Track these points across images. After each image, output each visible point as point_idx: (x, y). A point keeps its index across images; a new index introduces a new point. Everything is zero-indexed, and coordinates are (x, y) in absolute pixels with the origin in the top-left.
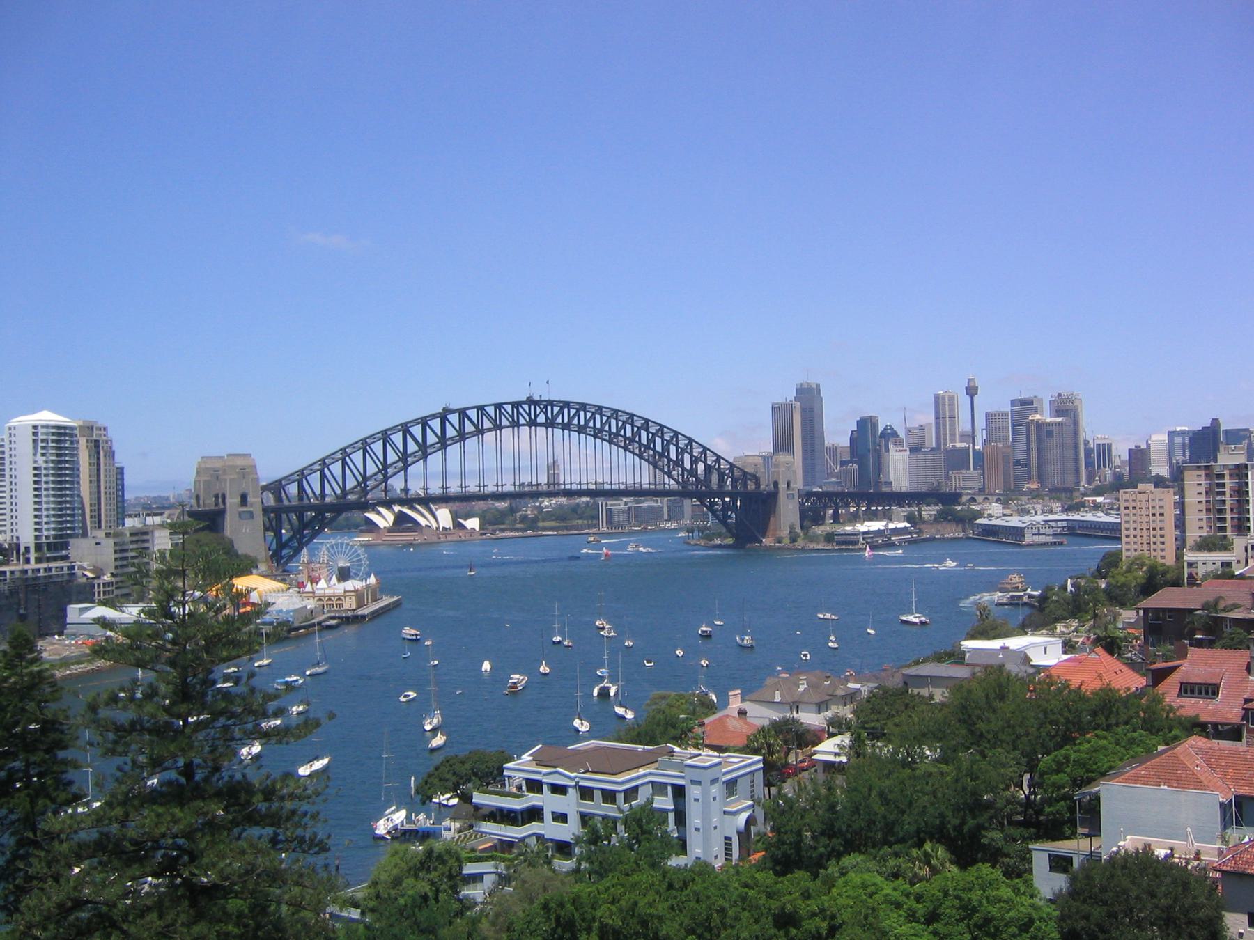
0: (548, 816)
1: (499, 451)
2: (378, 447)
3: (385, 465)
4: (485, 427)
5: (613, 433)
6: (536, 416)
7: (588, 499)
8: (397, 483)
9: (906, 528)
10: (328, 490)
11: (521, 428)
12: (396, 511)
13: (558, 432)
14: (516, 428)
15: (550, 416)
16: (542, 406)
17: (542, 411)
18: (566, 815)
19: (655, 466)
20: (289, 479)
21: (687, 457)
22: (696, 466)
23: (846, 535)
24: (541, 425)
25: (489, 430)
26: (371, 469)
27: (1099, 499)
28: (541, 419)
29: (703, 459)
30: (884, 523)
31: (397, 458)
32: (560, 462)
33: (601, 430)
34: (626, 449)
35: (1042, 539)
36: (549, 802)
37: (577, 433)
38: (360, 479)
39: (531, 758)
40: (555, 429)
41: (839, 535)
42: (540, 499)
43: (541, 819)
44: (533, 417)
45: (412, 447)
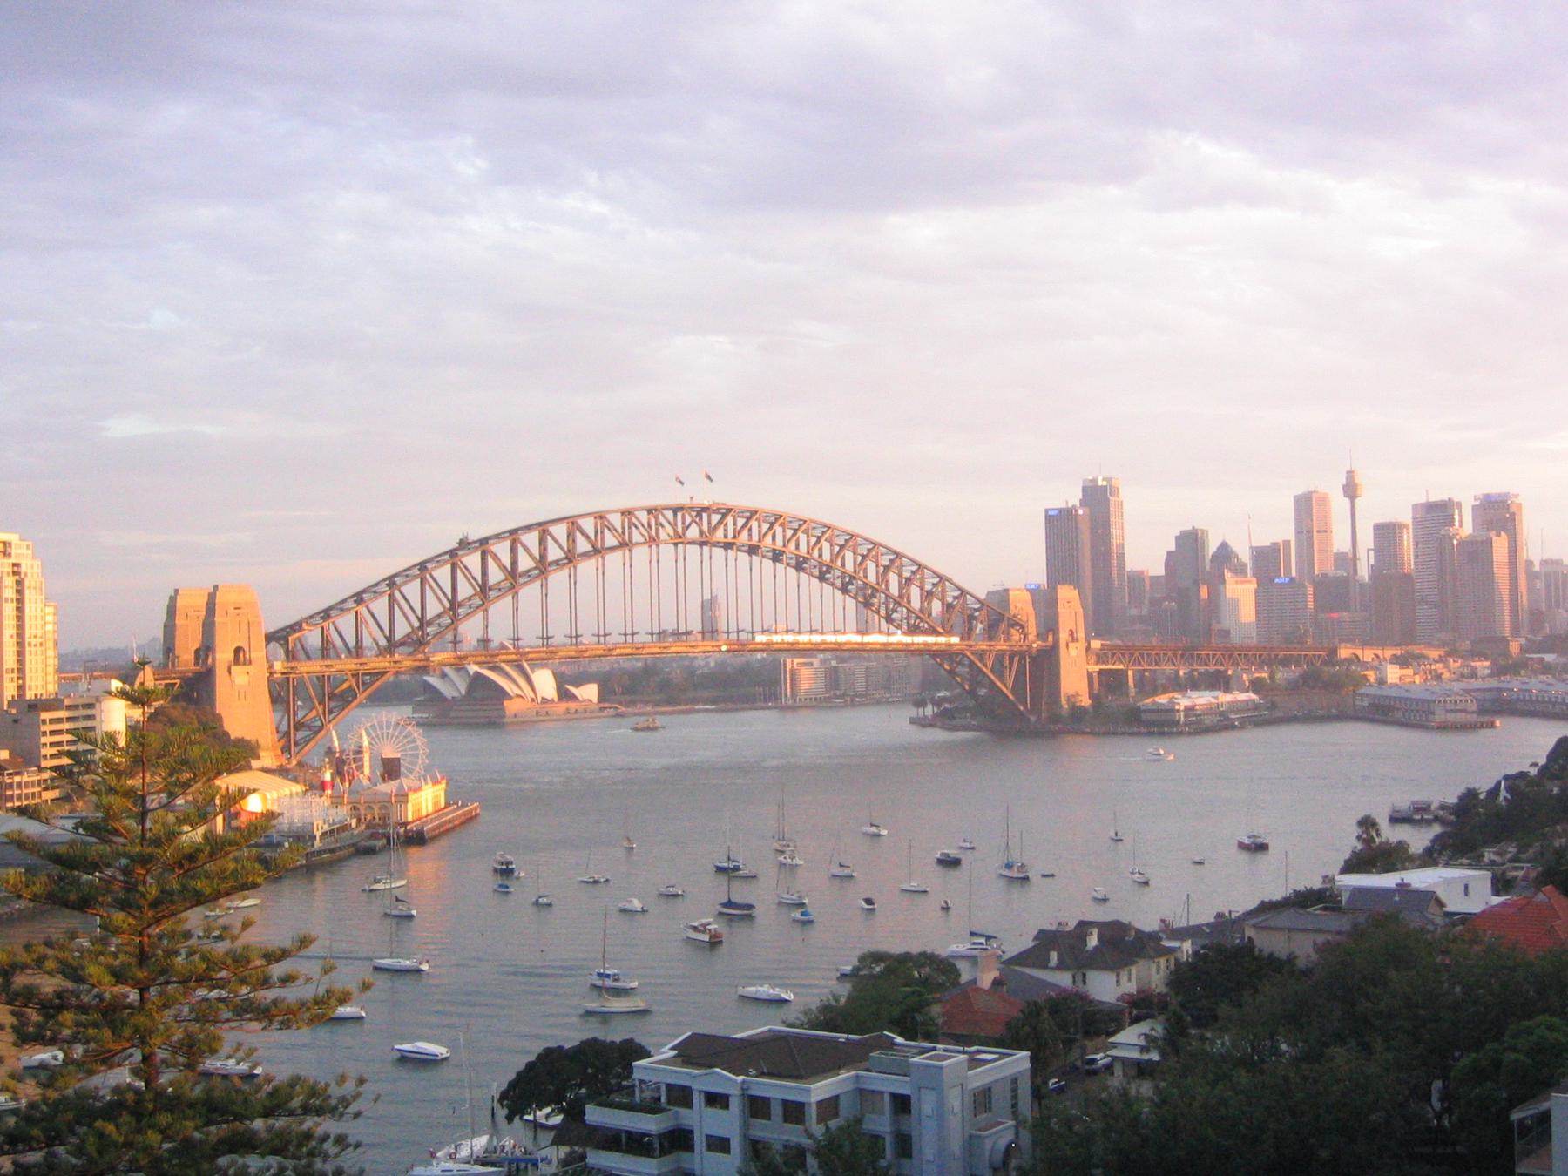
0: (699, 1141)
2: (443, 574)
3: (454, 604)
8: (471, 629)
12: (471, 673)
13: (718, 553)
14: (654, 547)
18: (728, 1140)
21: (915, 593)
23: (1158, 711)
24: (692, 543)
25: (612, 549)
26: (433, 608)
27: (1550, 658)
28: (693, 533)
32: (722, 600)
35: (1461, 718)
36: (703, 1121)
38: (416, 624)
39: (675, 1052)
44: (680, 529)
45: (495, 575)
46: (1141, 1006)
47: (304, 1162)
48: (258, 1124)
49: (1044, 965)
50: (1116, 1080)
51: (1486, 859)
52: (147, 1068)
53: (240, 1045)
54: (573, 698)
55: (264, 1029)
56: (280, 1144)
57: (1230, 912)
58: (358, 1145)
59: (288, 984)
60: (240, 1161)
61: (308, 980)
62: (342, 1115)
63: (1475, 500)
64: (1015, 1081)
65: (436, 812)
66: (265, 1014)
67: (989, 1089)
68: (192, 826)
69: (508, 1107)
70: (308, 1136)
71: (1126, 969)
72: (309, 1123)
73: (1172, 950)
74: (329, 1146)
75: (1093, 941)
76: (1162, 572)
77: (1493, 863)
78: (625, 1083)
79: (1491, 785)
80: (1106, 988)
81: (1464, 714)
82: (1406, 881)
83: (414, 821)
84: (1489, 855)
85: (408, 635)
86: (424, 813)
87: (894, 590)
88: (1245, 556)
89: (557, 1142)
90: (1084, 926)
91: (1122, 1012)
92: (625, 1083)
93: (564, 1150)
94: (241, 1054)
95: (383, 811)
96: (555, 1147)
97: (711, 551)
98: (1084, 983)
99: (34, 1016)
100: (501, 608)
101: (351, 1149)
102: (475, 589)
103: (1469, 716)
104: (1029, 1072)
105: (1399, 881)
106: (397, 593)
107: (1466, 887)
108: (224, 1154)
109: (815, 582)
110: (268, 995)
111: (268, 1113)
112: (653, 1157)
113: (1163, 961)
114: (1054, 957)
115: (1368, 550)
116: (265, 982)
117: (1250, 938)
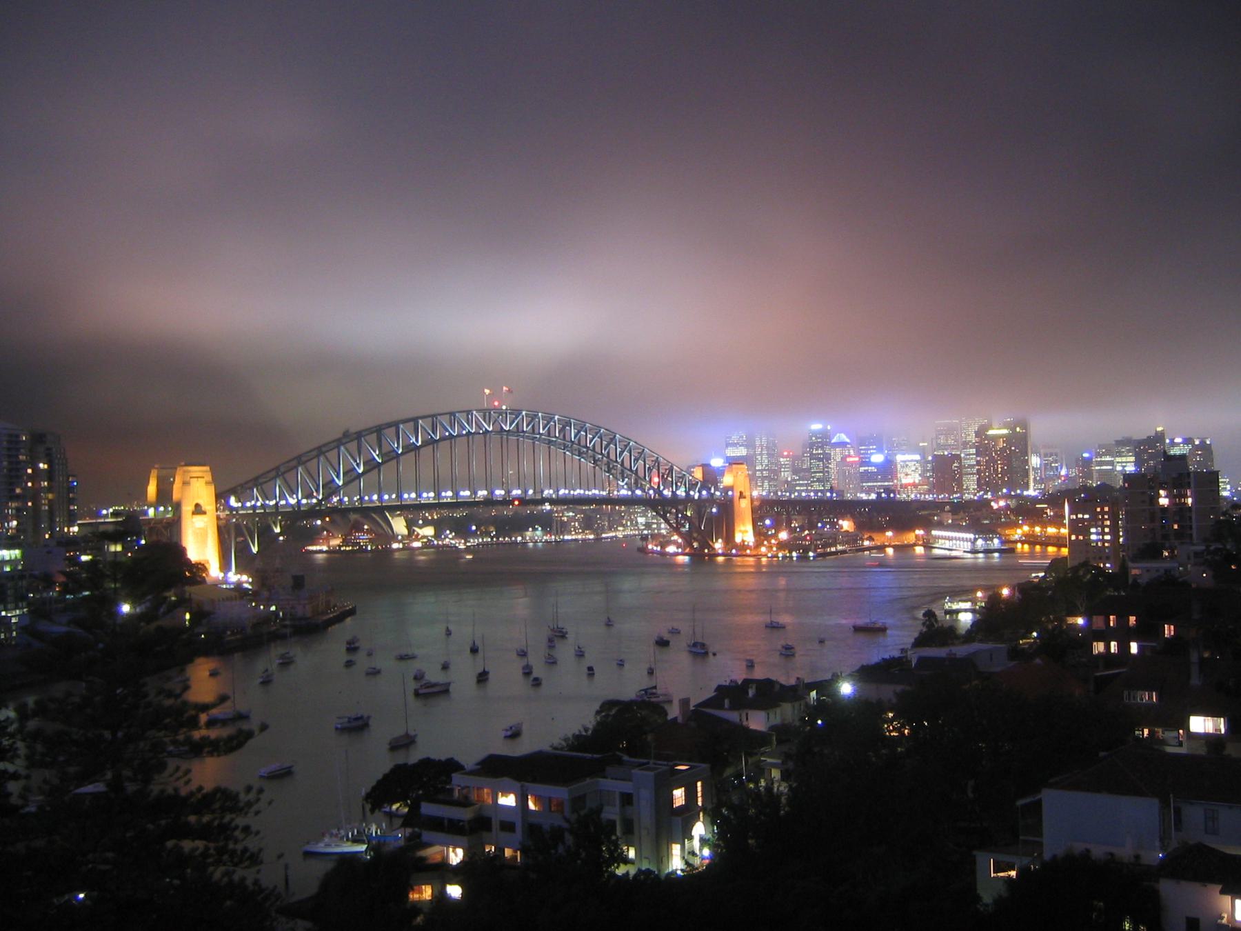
0: (495, 825)
46: (782, 732)
48: (192, 819)
49: (721, 707)
56: (203, 832)
58: (257, 833)
62: (246, 813)
74: (237, 833)
75: (751, 692)
90: (747, 682)
94: (180, 773)
99: (39, 748)
107: (991, 655)
111: (198, 811)
112: (465, 835)
113: (797, 704)
114: (727, 702)
115: (932, 439)
116: (193, 723)
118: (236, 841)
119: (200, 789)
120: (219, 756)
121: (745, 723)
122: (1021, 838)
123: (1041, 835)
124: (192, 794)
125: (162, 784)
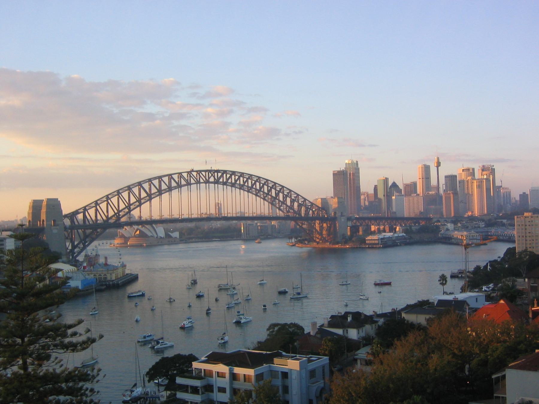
0: (215, 390)
1: (199, 198)
3: (130, 205)
4: (182, 184)
5: (250, 187)
6: (209, 178)
7: (237, 221)
8: (135, 213)
9: (403, 236)
10: (99, 217)
11: (192, 186)
13: (221, 186)
14: (198, 185)
15: (216, 178)
16: (212, 173)
17: (212, 175)
19: (272, 204)
20: (77, 212)
21: (288, 200)
22: (293, 204)
24: (212, 183)
25: (184, 185)
28: (212, 179)
29: (297, 201)
30: (392, 234)
31: (136, 200)
33: (243, 185)
34: (256, 195)
37: (230, 187)
38: (116, 211)
40: (219, 185)
41: (368, 240)
42: (212, 222)
43: (212, 391)
44: (207, 178)
45: (143, 194)
46: (367, 341)
47: (79, 398)
50: (359, 366)
51: (483, 290)
52: (24, 367)
53: (56, 358)
54: (170, 237)
55: (65, 352)
56: (70, 392)
57: (397, 308)
58: (98, 392)
59: (73, 336)
60: (57, 398)
61: (81, 335)
62: (92, 382)
63: (479, 167)
64: (323, 367)
65: (123, 276)
66: (66, 347)
67: (315, 370)
68: (39, 282)
69: (149, 378)
70: (81, 388)
71: (362, 328)
72: (81, 384)
73: (377, 322)
74: (87, 392)
75: (349, 319)
76: (373, 193)
77: (485, 291)
78: (189, 369)
79: (485, 264)
80: (353, 334)
81: (476, 240)
82: (456, 297)
83: (115, 280)
84: (484, 288)
85: (113, 216)
86: (119, 277)
87: (281, 199)
88: (401, 187)
89: (166, 390)
90: (347, 313)
91: (360, 342)
92: (189, 369)
93: (169, 392)
95: (105, 276)
96: (165, 391)
97: (218, 186)
98: (347, 333)
100: (145, 207)
101: (96, 393)
102: (137, 200)
103: (477, 241)
104: (328, 364)
105: (454, 297)
106: (109, 201)
107: (477, 299)
108: (51, 396)
109: (254, 196)
110: (67, 340)
111: (67, 381)
113: (374, 325)
115: (443, 185)
116: (65, 336)
117: (403, 317)
118: (87, 396)
119: (66, 369)
120: (77, 352)
121: (346, 335)
122: (495, 395)
123: (506, 394)
124: (63, 372)
125: (48, 367)
